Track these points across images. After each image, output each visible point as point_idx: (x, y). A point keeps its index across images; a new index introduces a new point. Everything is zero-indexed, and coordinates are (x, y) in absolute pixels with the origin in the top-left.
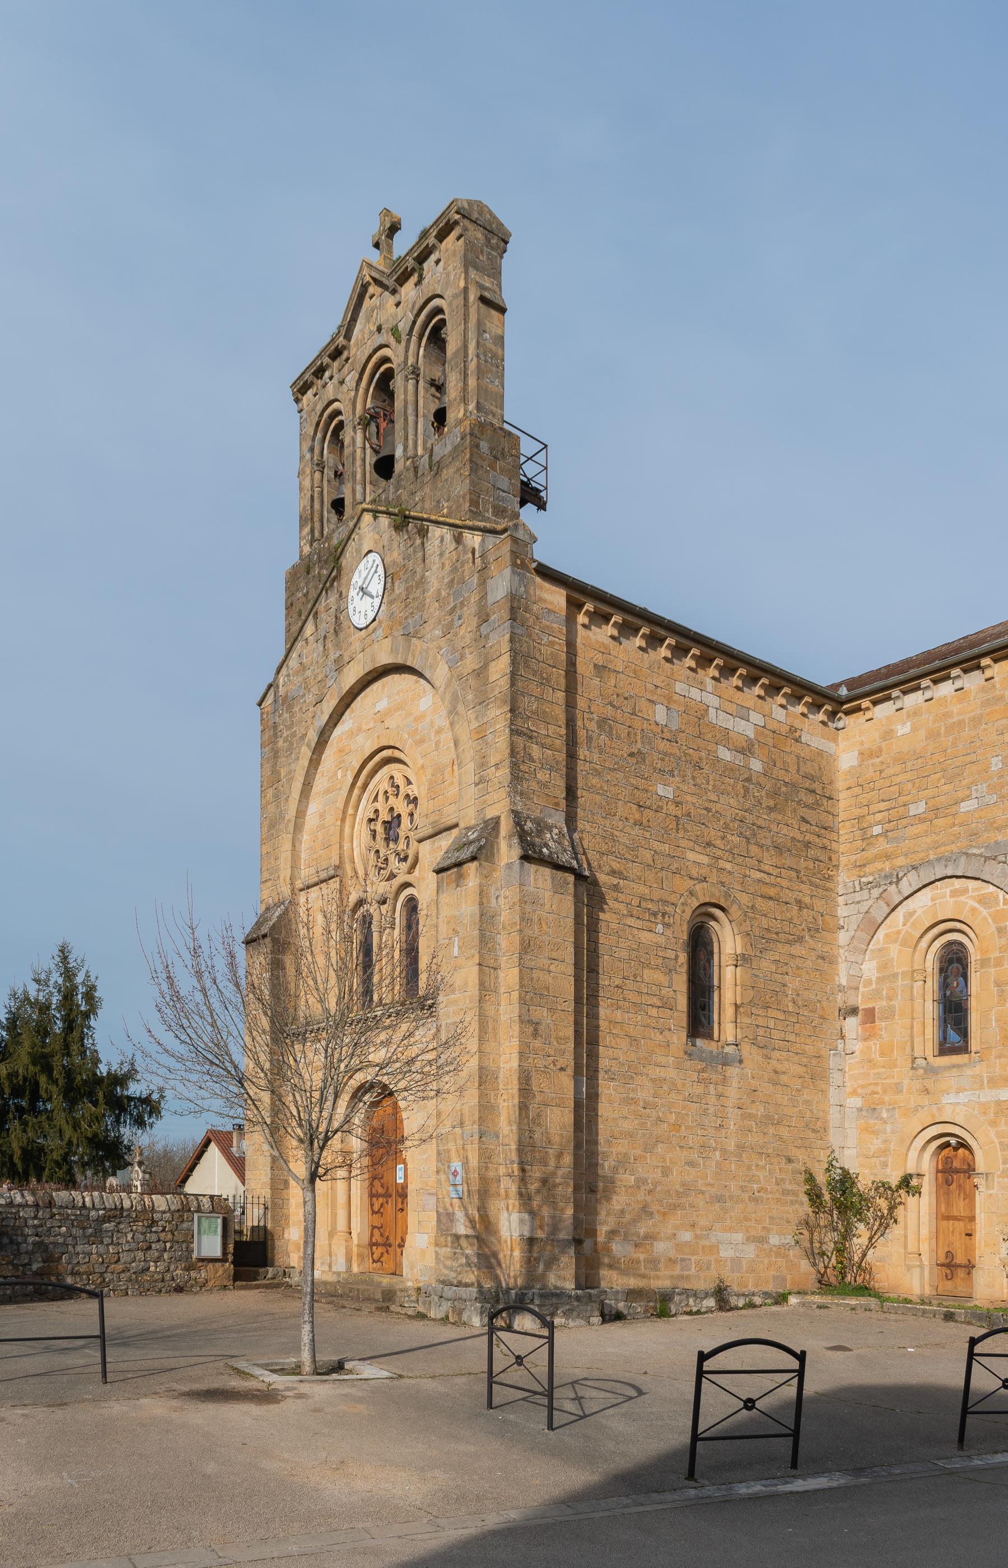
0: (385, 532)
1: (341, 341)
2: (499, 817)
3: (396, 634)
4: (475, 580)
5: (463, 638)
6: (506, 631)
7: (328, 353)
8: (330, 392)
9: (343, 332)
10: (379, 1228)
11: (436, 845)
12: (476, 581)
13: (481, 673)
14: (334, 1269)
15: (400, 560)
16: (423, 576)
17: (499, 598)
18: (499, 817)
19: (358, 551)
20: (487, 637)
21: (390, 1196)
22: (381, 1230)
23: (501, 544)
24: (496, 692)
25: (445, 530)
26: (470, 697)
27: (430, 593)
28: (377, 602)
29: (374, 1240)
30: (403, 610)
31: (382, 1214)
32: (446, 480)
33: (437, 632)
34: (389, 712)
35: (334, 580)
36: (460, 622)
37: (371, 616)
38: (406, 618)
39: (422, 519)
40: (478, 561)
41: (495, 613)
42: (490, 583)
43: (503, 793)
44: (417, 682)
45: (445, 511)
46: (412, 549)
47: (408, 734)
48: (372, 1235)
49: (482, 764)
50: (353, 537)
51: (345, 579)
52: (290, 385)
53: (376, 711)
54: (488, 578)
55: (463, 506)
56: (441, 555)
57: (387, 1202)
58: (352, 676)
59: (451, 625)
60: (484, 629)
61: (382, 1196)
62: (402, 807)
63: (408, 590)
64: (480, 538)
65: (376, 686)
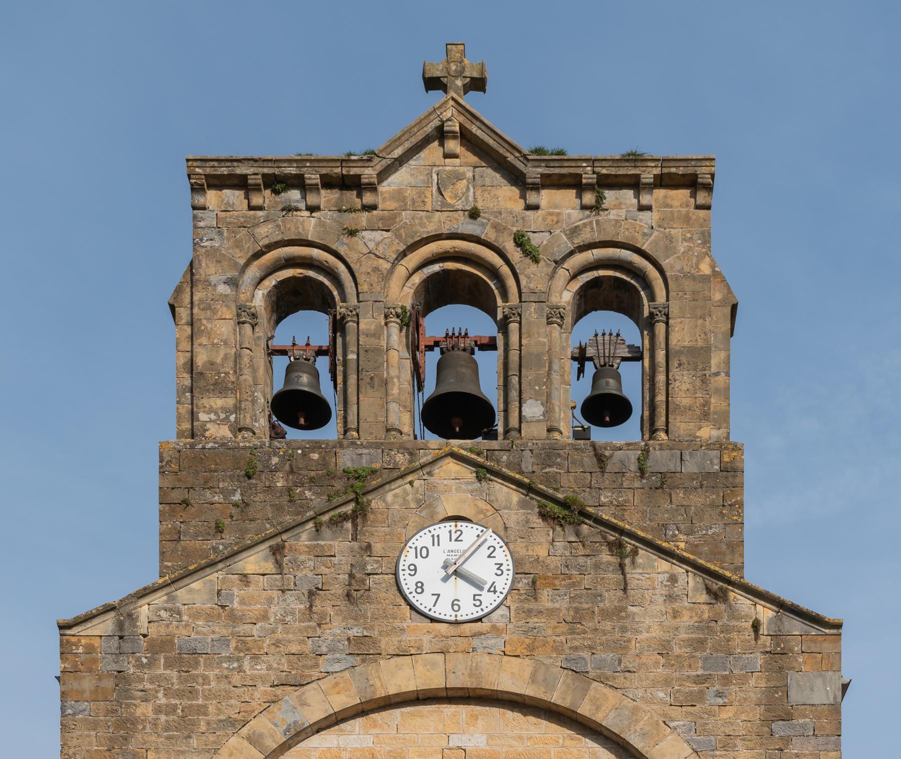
5: (728, 723)
12: (760, 662)
23: (820, 638)
25: (679, 570)
30: (563, 633)
33: (661, 695)
36: (720, 701)
41: (805, 716)
50: (409, 478)
54: (789, 669)
59: (700, 696)
64: (771, 614)
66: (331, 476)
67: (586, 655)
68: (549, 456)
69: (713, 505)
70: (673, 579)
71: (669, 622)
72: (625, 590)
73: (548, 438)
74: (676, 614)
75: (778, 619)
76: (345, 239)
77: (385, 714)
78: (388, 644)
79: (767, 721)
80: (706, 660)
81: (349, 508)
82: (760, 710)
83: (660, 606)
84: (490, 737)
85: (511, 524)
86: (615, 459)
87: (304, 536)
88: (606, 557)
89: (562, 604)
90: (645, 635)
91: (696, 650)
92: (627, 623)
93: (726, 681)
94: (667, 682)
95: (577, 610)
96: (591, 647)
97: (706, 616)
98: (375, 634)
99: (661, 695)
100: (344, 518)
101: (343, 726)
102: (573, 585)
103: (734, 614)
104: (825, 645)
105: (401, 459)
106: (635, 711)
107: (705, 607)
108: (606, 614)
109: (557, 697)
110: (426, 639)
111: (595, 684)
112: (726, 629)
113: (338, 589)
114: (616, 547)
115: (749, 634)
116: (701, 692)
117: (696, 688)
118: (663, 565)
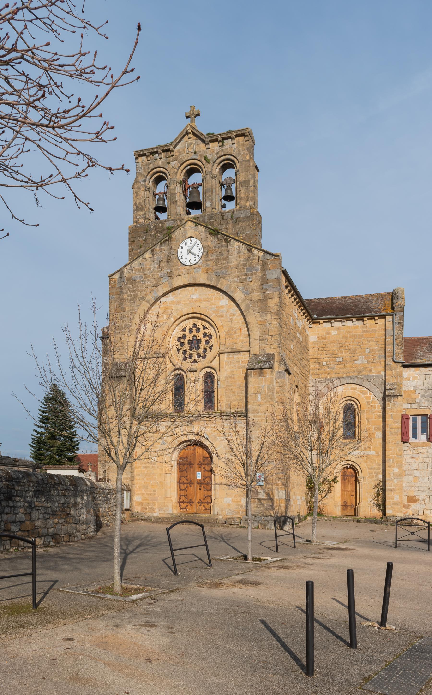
0: (202, 233)
1: (171, 148)
2: (274, 354)
3: (209, 273)
4: (260, 267)
5: (252, 286)
6: (277, 290)
7: (162, 149)
8: (160, 162)
9: (174, 145)
10: (184, 496)
11: (231, 356)
13: (264, 301)
14: (167, 512)
15: (212, 246)
16: (228, 257)
17: (273, 278)
18: (274, 354)
19: (184, 234)
20: (266, 290)
21: (193, 484)
22: (187, 497)
24: (272, 310)
25: (241, 244)
26: (257, 308)
27: (232, 264)
28: (198, 258)
29: (181, 500)
31: (187, 491)
32: (242, 226)
33: (236, 280)
34: (200, 300)
35: (166, 240)
36: (250, 280)
37: (193, 262)
38: (217, 269)
39: (227, 236)
40: (261, 261)
42: (268, 272)
43: (275, 346)
44: (218, 293)
45: (241, 237)
46: (220, 245)
47: (213, 312)
48: (180, 499)
49: (264, 333)
51: (175, 242)
52: (135, 151)
53: (191, 298)
55: (252, 240)
56: (239, 252)
57: (191, 486)
58: (178, 282)
60: (264, 286)
61: (188, 484)
62: (200, 335)
63: (218, 260)
64: (262, 254)
65: (190, 288)
66: (164, 229)
67: (219, 271)
68: (211, 217)
69: (249, 225)
70: (239, 247)
71: (238, 259)
72: (228, 252)
73: (212, 211)
74: (240, 257)
75: (264, 255)
76: (167, 165)
77: (177, 291)
78: (176, 273)
79: (261, 285)
80: (247, 269)
81: (167, 238)
82: (260, 282)
83: (236, 255)
84: (200, 295)
85: (203, 237)
86: (226, 216)
87: (158, 246)
88: (224, 243)
89: (214, 257)
90: (233, 264)
91: (245, 266)
92: (229, 261)
93: (252, 274)
94: (238, 276)
95: (217, 259)
96: (220, 269)
97: (247, 256)
98: (173, 271)
99: (236, 280)
100: (166, 240)
101: (168, 295)
102: (216, 252)
103: (254, 255)
104: (276, 261)
105: (179, 223)
106: (230, 285)
107: (247, 254)
108: (224, 259)
109: (213, 284)
110: (184, 270)
111: (221, 279)
112: (252, 260)
113: (165, 260)
114: (226, 240)
115: (257, 261)
116: (246, 278)
117: (244, 277)
118: (237, 244)
